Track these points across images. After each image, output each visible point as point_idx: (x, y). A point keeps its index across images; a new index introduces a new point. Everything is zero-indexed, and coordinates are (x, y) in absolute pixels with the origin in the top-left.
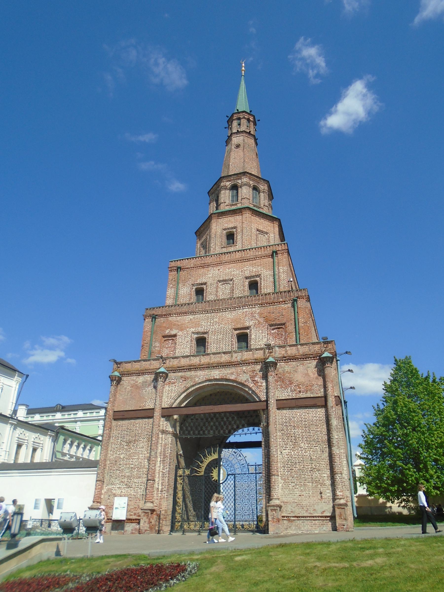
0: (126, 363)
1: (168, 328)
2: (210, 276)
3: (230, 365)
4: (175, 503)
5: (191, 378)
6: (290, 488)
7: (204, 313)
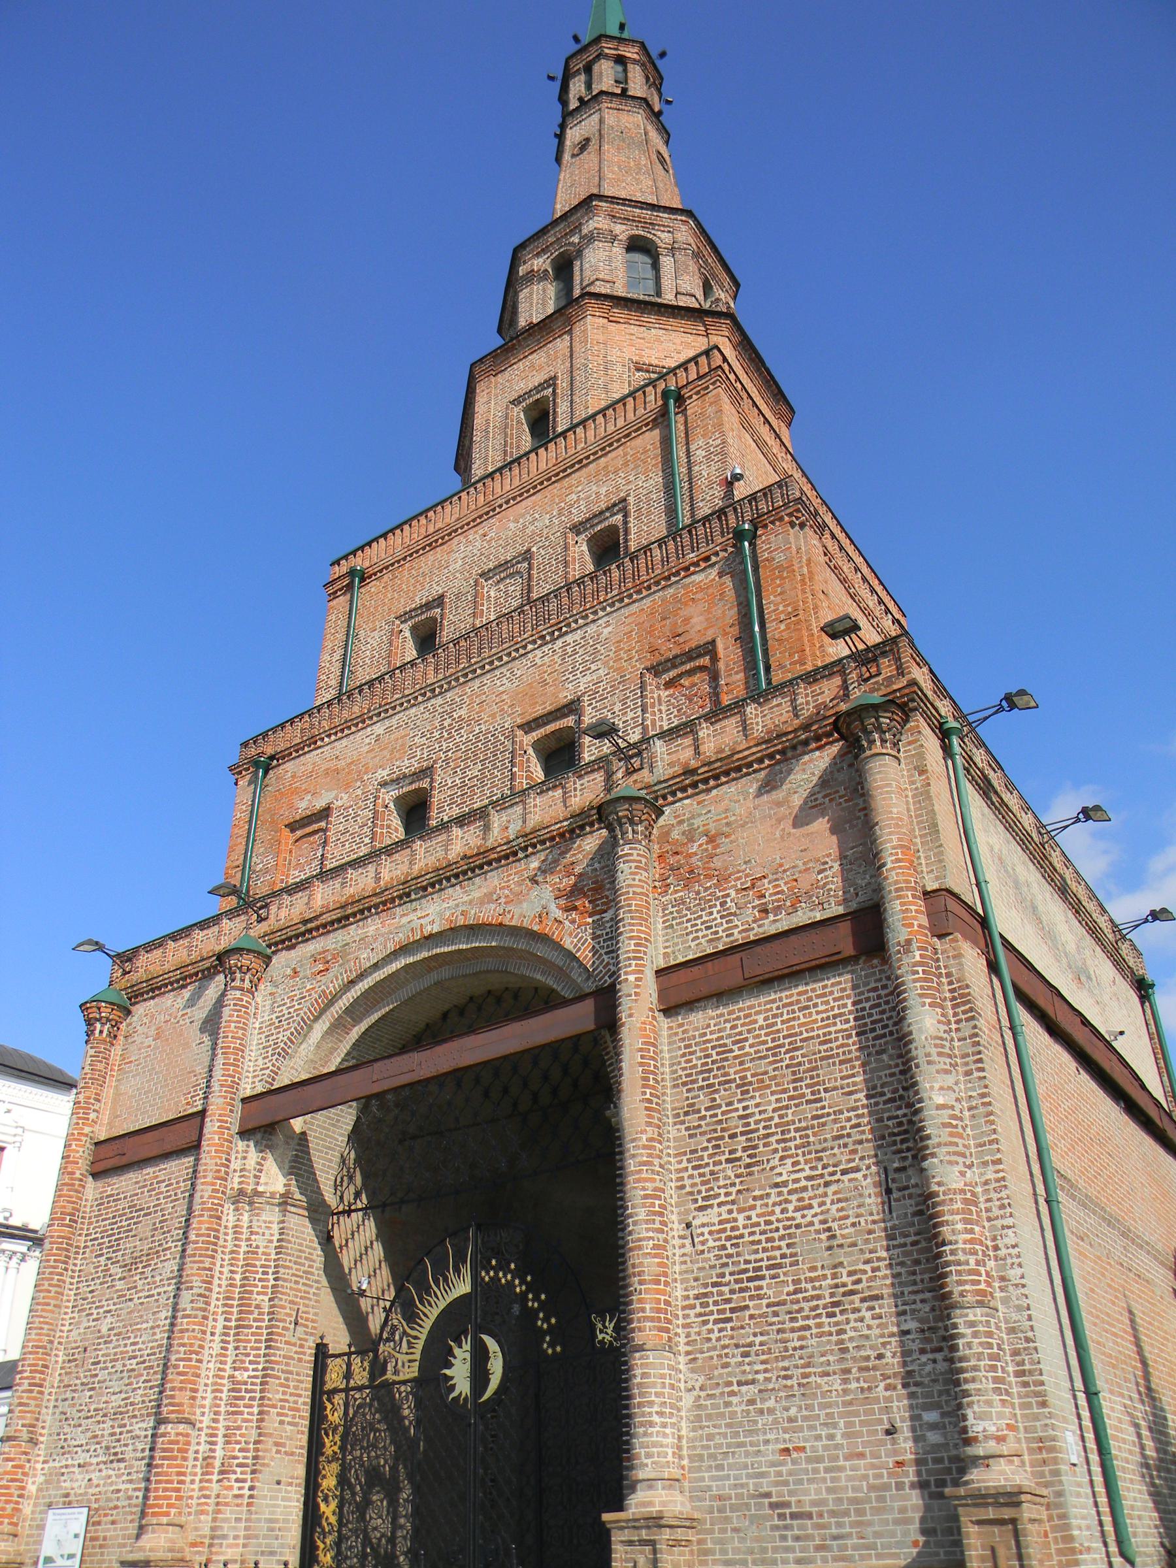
0: (150, 947)
3: (481, 867)
4: (311, 1518)
5: (342, 953)
6: (733, 1414)
7: (420, 699)
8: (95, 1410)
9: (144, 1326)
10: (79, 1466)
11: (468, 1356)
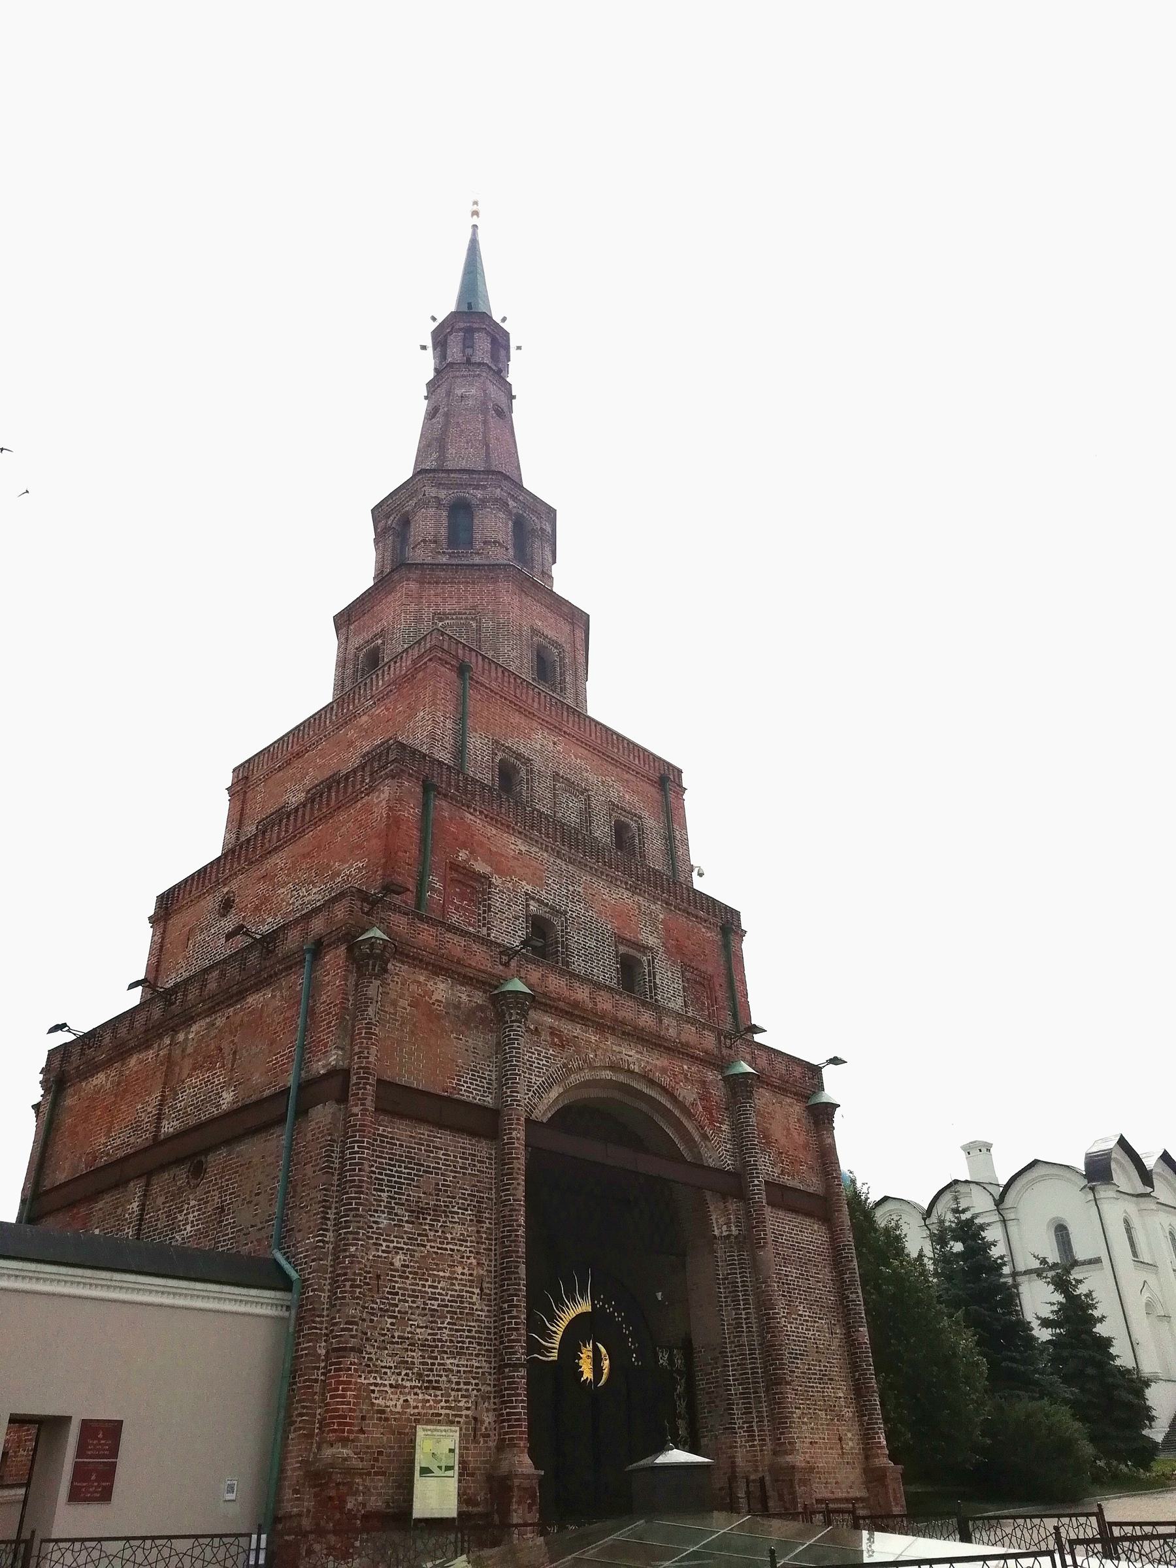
1: (464, 846)
2: (539, 745)
8: (399, 1337)
9: (441, 1274)
10: (391, 1386)
11: (591, 1354)
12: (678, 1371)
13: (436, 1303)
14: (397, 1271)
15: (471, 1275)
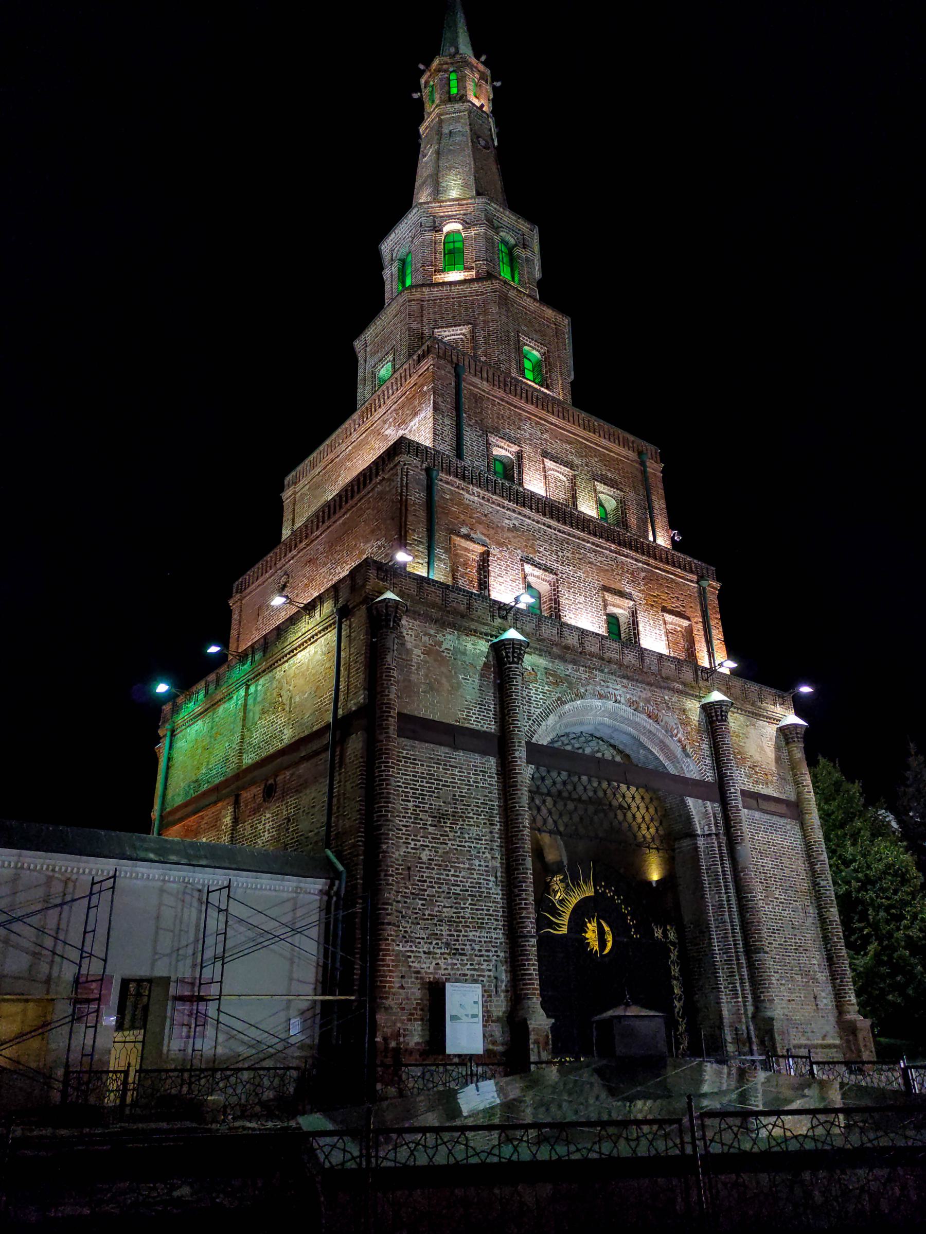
1: (464, 523)
8: (429, 915)
9: (462, 866)
10: (425, 952)
12: (673, 944)
13: (458, 888)
14: (424, 863)
15: (487, 866)
